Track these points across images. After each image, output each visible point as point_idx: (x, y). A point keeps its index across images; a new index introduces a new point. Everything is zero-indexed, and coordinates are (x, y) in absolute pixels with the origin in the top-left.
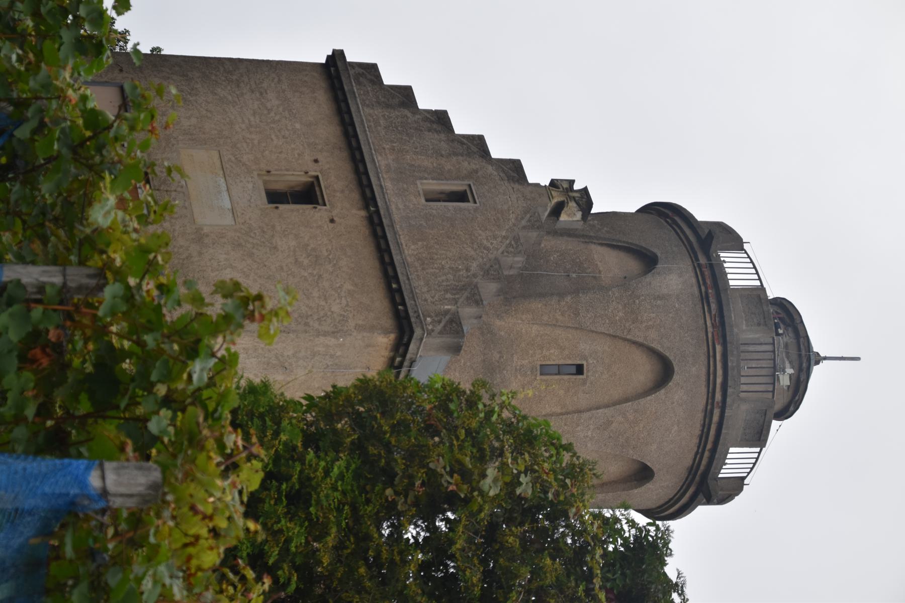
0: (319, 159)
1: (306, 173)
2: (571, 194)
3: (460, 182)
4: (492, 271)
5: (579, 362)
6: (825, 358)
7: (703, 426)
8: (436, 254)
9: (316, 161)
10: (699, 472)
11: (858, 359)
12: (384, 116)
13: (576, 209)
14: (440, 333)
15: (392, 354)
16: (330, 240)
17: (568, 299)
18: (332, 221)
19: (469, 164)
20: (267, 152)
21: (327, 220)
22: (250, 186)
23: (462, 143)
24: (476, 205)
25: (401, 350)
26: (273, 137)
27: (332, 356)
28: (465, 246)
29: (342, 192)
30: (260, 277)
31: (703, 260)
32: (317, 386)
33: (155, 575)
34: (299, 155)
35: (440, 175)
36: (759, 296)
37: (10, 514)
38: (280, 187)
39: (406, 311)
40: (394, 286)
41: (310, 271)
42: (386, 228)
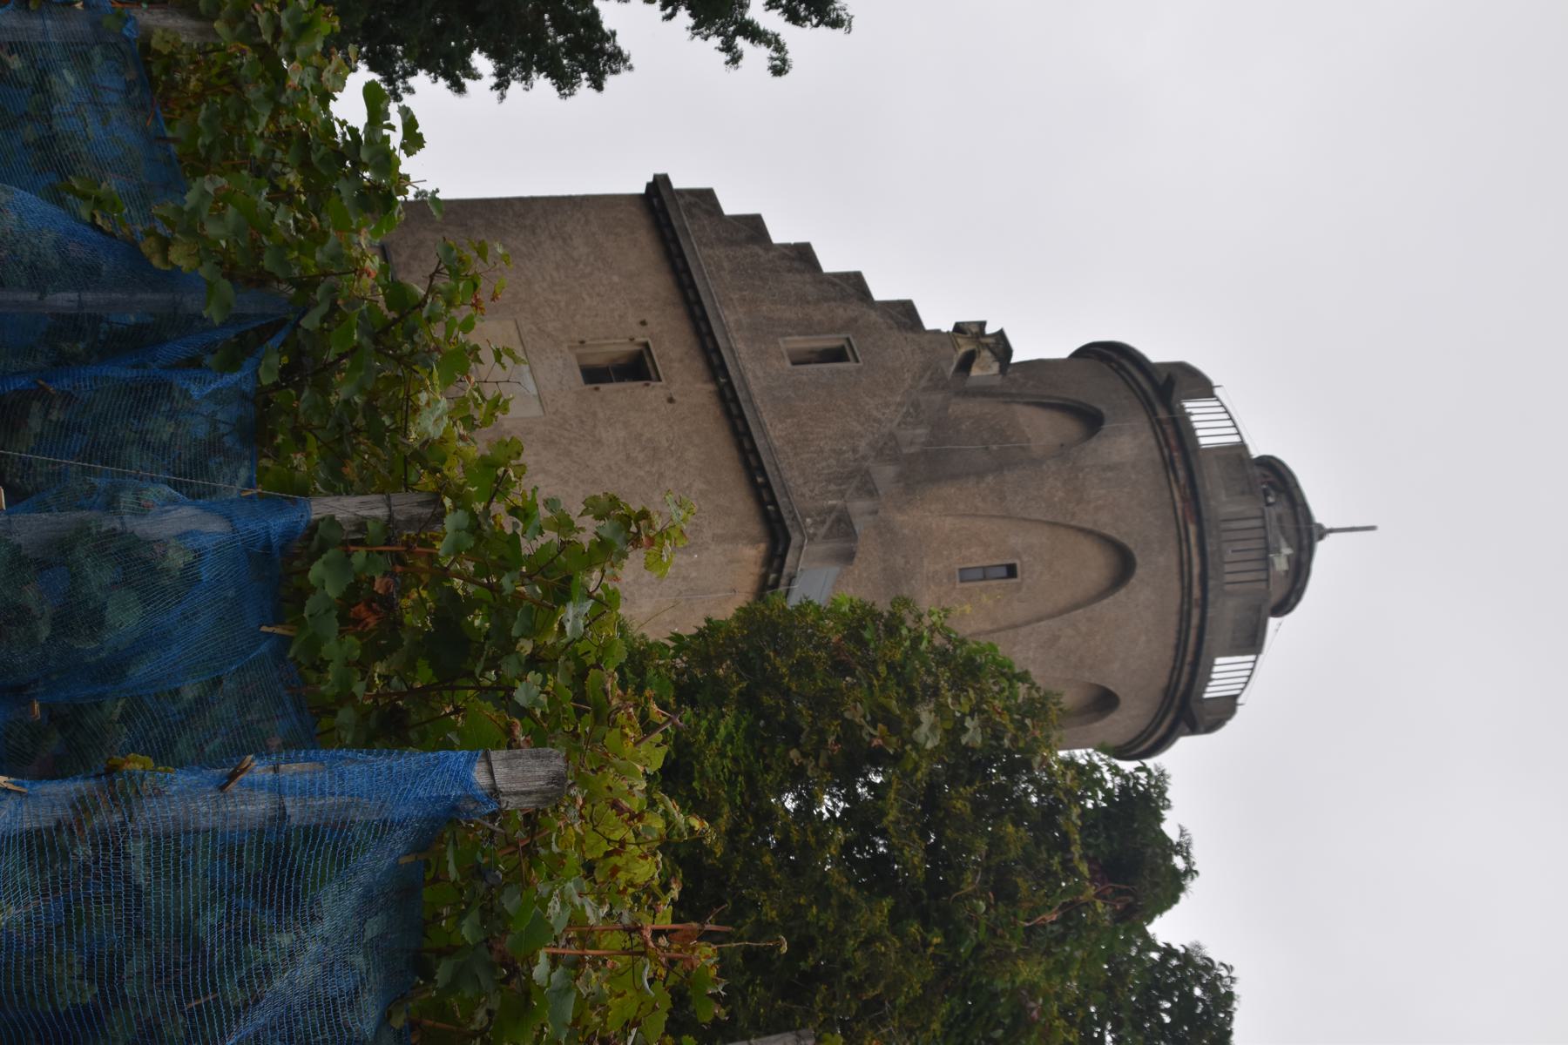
0: (647, 320)
1: (632, 340)
2: (984, 340)
3: (836, 336)
4: (888, 450)
5: (1010, 562)
6: (1332, 531)
7: (1180, 632)
8: (812, 434)
9: (643, 323)
10: (1179, 694)
11: (1372, 528)
12: (727, 256)
13: (991, 360)
14: (826, 537)
15: (764, 570)
16: (670, 426)
17: (990, 479)
18: (671, 400)
19: (845, 310)
20: (578, 317)
21: (665, 400)
22: (559, 363)
23: (834, 285)
24: (855, 364)
25: (776, 564)
26: (585, 296)
27: (684, 579)
28: (849, 419)
29: (681, 361)
30: (582, 481)
31: (1162, 414)
32: (668, 619)
33: (562, 892)
34: (620, 316)
35: (807, 328)
36: (1239, 456)
37: (377, 826)
38: (597, 360)
39: (778, 511)
40: (760, 480)
41: (647, 468)
42: (743, 405)
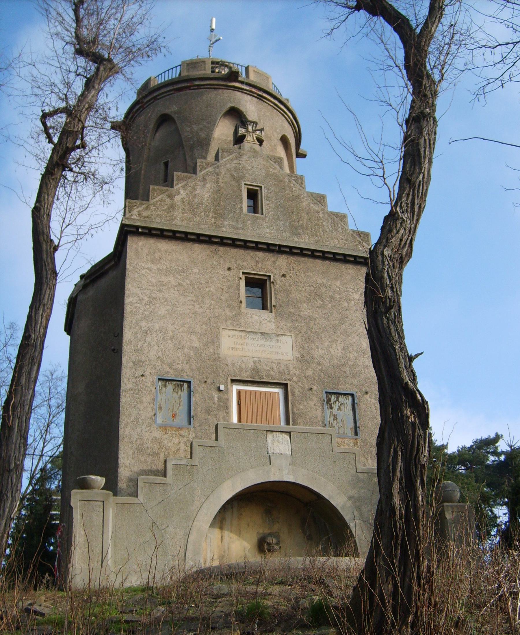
9: (229, 269)
41: (328, 303)
